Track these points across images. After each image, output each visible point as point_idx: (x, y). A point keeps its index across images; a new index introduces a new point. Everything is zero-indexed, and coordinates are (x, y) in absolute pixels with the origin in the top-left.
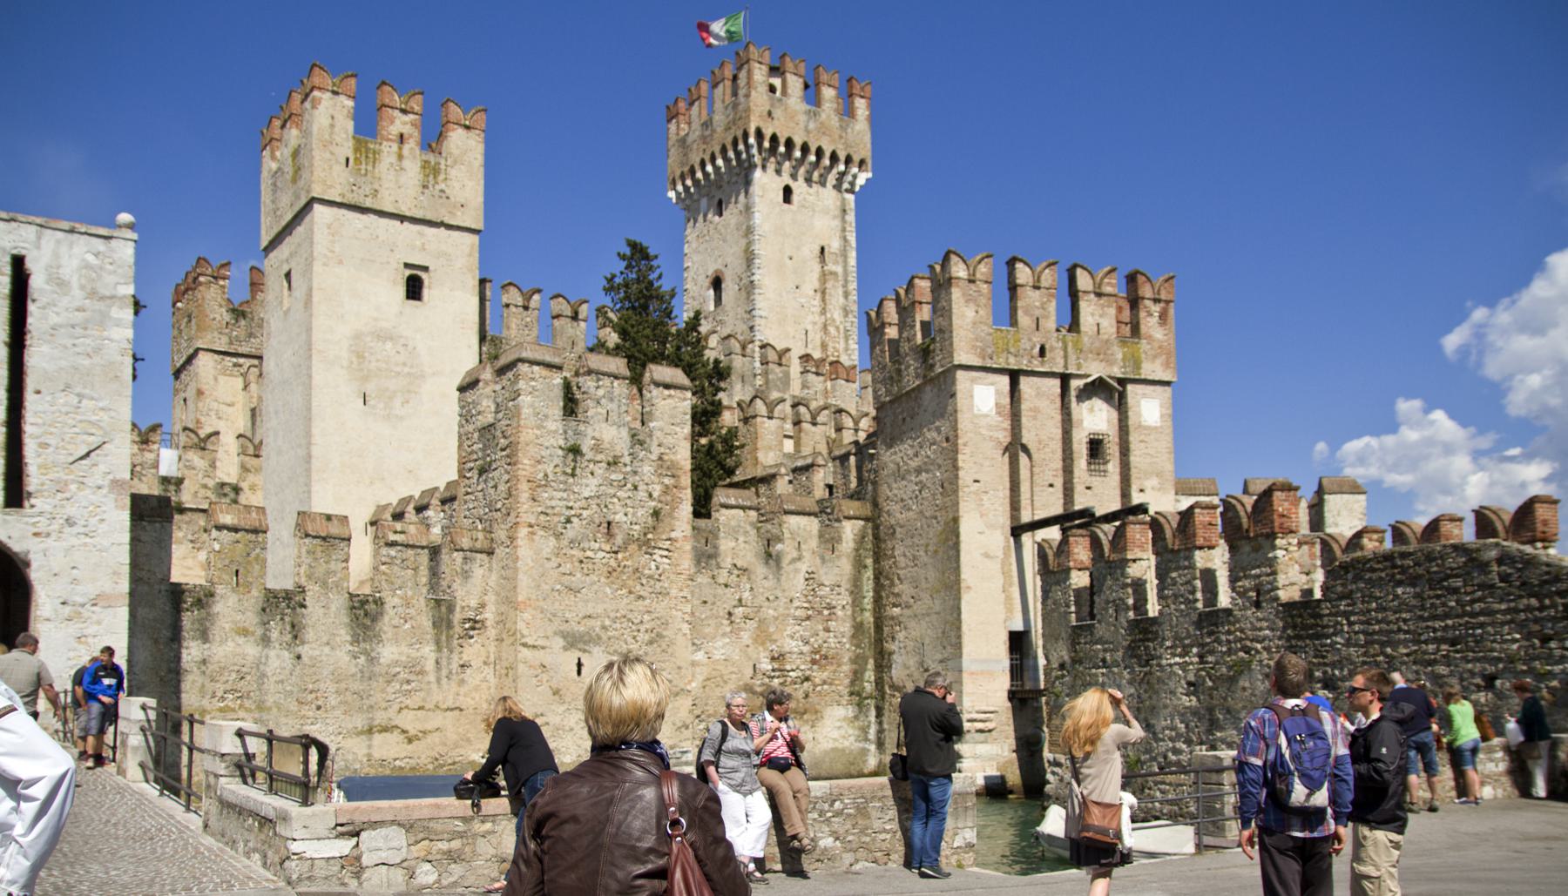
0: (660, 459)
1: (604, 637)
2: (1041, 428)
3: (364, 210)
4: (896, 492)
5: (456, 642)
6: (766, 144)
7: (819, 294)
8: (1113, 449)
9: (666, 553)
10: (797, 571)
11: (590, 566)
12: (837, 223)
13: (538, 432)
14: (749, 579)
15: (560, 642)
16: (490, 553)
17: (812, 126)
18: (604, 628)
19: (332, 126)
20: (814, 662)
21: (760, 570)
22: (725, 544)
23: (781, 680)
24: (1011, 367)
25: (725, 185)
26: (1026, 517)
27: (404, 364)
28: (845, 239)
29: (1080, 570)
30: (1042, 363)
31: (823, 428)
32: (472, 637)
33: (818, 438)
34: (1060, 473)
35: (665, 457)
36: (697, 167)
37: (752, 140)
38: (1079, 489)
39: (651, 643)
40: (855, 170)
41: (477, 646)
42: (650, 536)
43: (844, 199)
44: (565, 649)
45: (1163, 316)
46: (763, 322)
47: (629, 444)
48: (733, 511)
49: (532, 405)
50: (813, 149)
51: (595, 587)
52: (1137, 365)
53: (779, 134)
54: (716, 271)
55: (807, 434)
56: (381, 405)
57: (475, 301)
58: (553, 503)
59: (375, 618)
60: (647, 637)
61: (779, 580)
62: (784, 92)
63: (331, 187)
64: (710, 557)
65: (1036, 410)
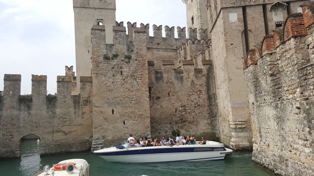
0: (137, 53)
9: (140, 78)
10: (188, 81)
14: (173, 84)
16: (92, 82)
18: (121, 100)
20: (195, 107)
21: (176, 82)
22: (165, 76)
32: (87, 105)
35: (138, 52)
42: (135, 74)
48: (167, 66)
49: (96, 41)
58: (104, 67)
64: (160, 79)
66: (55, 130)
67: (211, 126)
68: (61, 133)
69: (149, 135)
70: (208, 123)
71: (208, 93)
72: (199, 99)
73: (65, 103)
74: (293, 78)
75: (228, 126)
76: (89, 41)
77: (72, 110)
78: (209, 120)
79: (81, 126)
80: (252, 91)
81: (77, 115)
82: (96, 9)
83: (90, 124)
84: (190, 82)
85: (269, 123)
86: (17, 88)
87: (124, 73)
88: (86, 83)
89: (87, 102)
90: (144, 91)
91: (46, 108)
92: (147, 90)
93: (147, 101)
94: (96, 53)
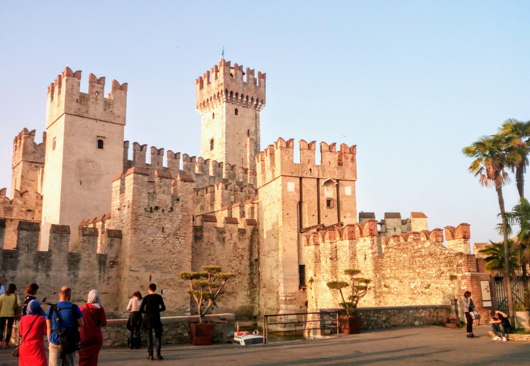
0: (182, 206)
1: (160, 267)
2: (310, 197)
3: (83, 117)
6: (229, 95)
8: (334, 203)
9: (183, 238)
10: (230, 243)
12: (254, 121)
13: (139, 197)
14: (213, 246)
15: (143, 269)
18: (160, 264)
19: (72, 88)
21: (217, 243)
22: (206, 234)
24: (300, 176)
25: (215, 107)
27: (96, 171)
28: (256, 127)
30: (311, 175)
31: (244, 193)
32: (113, 267)
34: (317, 211)
37: (223, 93)
39: (176, 269)
40: (260, 104)
42: (178, 232)
43: (256, 114)
44: (146, 271)
46: (227, 155)
47: (171, 201)
48: (209, 223)
51: (157, 250)
53: (233, 91)
54: (212, 137)
55: (239, 195)
56: (87, 185)
57: (122, 149)
58: (144, 221)
59: (78, 261)
60: (175, 267)
61: (224, 246)
62: (236, 77)
63: (72, 109)
65: (308, 190)
67: (250, 298)
69: (188, 308)
70: (247, 295)
71: (250, 259)
72: (240, 265)
73: (89, 264)
74: (346, 265)
75: (275, 299)
76: (82, 167)
77: (96, 273)
78: (249, 291)
79: (105, 295)
80: (312, 267)
81: (102, 280)
82: (97, 120)
83: (116, 292)
84: (232, 244)
85: (325, 295)
86: (35, 241)
87: (166, 230)
88: (115, 238)
89: (114, 263)
90: (186, 253)
91: (67, 268)
93: (189, 266)
94: (136, 204)
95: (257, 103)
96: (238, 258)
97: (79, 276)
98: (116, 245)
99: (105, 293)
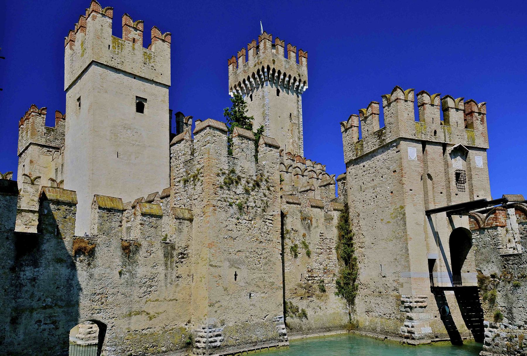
1: (247, 262)
4: (359, 198)
5: (174, 265)
6: (271, 72)
7: (290, 131)
9: (271, 221)
10: (316, 232)
11: (240, 227)
15: (227, 264)
17: (287, 66)
23: (312, 281)
26: (432, 207)
27: (136, 141)
29: (501, 227)
33: (304, 181)
36: (242, 82)
37: (266, 70)
38: (453, 194)
41: (185, 266)
45: (482, 120)
50: (288, 75)
51: (242, 237)
52: (473, 141)
53: (275, 69)
66: (133, 310)
68: (144, 317)
77: (161, 269)
81: (169, 281)
92: (279, 242)
93: (279, 260)
95: (299, 84)
96: (326, 251)
97: (138, 275)
98: (185, 229)
99: (174, 299)
